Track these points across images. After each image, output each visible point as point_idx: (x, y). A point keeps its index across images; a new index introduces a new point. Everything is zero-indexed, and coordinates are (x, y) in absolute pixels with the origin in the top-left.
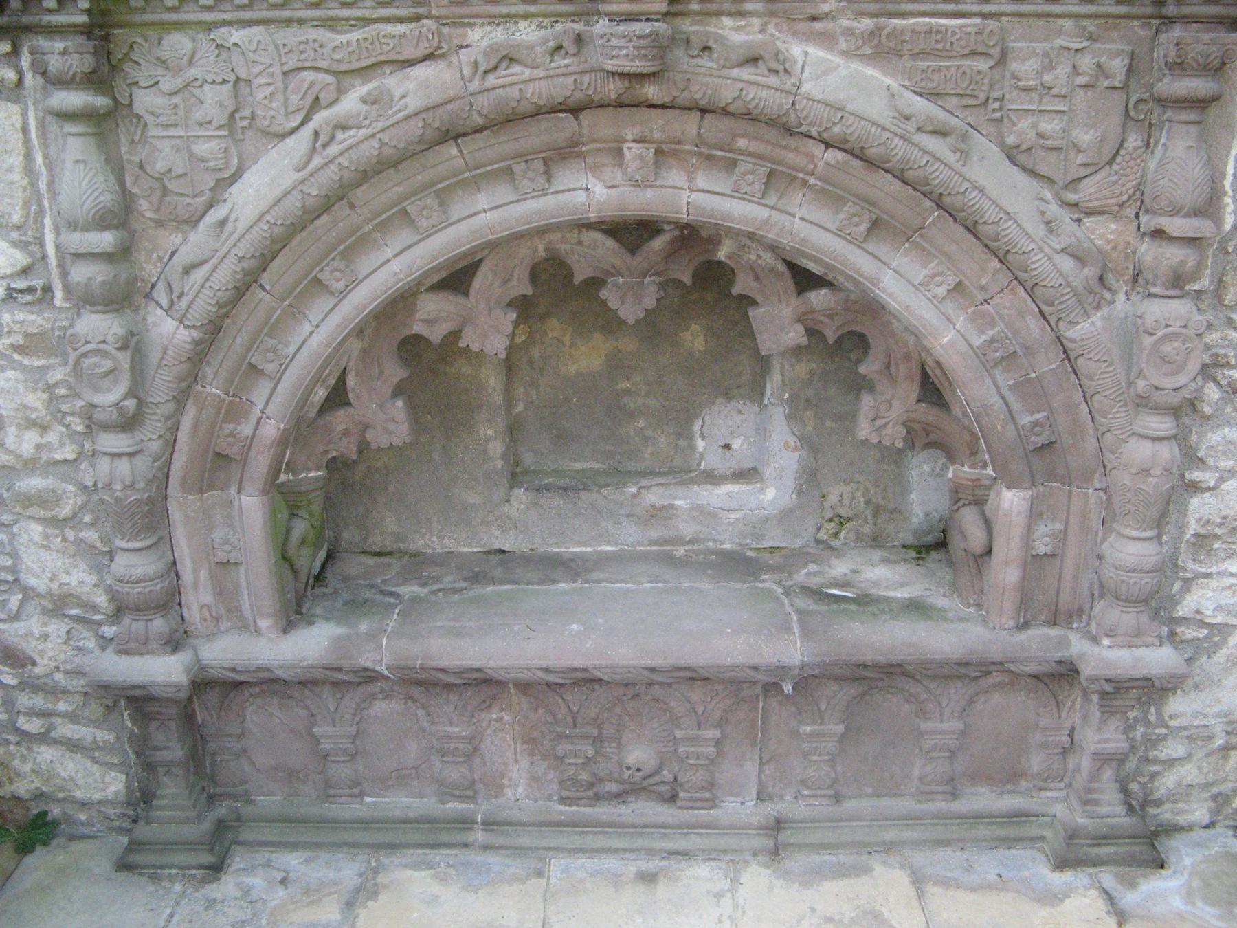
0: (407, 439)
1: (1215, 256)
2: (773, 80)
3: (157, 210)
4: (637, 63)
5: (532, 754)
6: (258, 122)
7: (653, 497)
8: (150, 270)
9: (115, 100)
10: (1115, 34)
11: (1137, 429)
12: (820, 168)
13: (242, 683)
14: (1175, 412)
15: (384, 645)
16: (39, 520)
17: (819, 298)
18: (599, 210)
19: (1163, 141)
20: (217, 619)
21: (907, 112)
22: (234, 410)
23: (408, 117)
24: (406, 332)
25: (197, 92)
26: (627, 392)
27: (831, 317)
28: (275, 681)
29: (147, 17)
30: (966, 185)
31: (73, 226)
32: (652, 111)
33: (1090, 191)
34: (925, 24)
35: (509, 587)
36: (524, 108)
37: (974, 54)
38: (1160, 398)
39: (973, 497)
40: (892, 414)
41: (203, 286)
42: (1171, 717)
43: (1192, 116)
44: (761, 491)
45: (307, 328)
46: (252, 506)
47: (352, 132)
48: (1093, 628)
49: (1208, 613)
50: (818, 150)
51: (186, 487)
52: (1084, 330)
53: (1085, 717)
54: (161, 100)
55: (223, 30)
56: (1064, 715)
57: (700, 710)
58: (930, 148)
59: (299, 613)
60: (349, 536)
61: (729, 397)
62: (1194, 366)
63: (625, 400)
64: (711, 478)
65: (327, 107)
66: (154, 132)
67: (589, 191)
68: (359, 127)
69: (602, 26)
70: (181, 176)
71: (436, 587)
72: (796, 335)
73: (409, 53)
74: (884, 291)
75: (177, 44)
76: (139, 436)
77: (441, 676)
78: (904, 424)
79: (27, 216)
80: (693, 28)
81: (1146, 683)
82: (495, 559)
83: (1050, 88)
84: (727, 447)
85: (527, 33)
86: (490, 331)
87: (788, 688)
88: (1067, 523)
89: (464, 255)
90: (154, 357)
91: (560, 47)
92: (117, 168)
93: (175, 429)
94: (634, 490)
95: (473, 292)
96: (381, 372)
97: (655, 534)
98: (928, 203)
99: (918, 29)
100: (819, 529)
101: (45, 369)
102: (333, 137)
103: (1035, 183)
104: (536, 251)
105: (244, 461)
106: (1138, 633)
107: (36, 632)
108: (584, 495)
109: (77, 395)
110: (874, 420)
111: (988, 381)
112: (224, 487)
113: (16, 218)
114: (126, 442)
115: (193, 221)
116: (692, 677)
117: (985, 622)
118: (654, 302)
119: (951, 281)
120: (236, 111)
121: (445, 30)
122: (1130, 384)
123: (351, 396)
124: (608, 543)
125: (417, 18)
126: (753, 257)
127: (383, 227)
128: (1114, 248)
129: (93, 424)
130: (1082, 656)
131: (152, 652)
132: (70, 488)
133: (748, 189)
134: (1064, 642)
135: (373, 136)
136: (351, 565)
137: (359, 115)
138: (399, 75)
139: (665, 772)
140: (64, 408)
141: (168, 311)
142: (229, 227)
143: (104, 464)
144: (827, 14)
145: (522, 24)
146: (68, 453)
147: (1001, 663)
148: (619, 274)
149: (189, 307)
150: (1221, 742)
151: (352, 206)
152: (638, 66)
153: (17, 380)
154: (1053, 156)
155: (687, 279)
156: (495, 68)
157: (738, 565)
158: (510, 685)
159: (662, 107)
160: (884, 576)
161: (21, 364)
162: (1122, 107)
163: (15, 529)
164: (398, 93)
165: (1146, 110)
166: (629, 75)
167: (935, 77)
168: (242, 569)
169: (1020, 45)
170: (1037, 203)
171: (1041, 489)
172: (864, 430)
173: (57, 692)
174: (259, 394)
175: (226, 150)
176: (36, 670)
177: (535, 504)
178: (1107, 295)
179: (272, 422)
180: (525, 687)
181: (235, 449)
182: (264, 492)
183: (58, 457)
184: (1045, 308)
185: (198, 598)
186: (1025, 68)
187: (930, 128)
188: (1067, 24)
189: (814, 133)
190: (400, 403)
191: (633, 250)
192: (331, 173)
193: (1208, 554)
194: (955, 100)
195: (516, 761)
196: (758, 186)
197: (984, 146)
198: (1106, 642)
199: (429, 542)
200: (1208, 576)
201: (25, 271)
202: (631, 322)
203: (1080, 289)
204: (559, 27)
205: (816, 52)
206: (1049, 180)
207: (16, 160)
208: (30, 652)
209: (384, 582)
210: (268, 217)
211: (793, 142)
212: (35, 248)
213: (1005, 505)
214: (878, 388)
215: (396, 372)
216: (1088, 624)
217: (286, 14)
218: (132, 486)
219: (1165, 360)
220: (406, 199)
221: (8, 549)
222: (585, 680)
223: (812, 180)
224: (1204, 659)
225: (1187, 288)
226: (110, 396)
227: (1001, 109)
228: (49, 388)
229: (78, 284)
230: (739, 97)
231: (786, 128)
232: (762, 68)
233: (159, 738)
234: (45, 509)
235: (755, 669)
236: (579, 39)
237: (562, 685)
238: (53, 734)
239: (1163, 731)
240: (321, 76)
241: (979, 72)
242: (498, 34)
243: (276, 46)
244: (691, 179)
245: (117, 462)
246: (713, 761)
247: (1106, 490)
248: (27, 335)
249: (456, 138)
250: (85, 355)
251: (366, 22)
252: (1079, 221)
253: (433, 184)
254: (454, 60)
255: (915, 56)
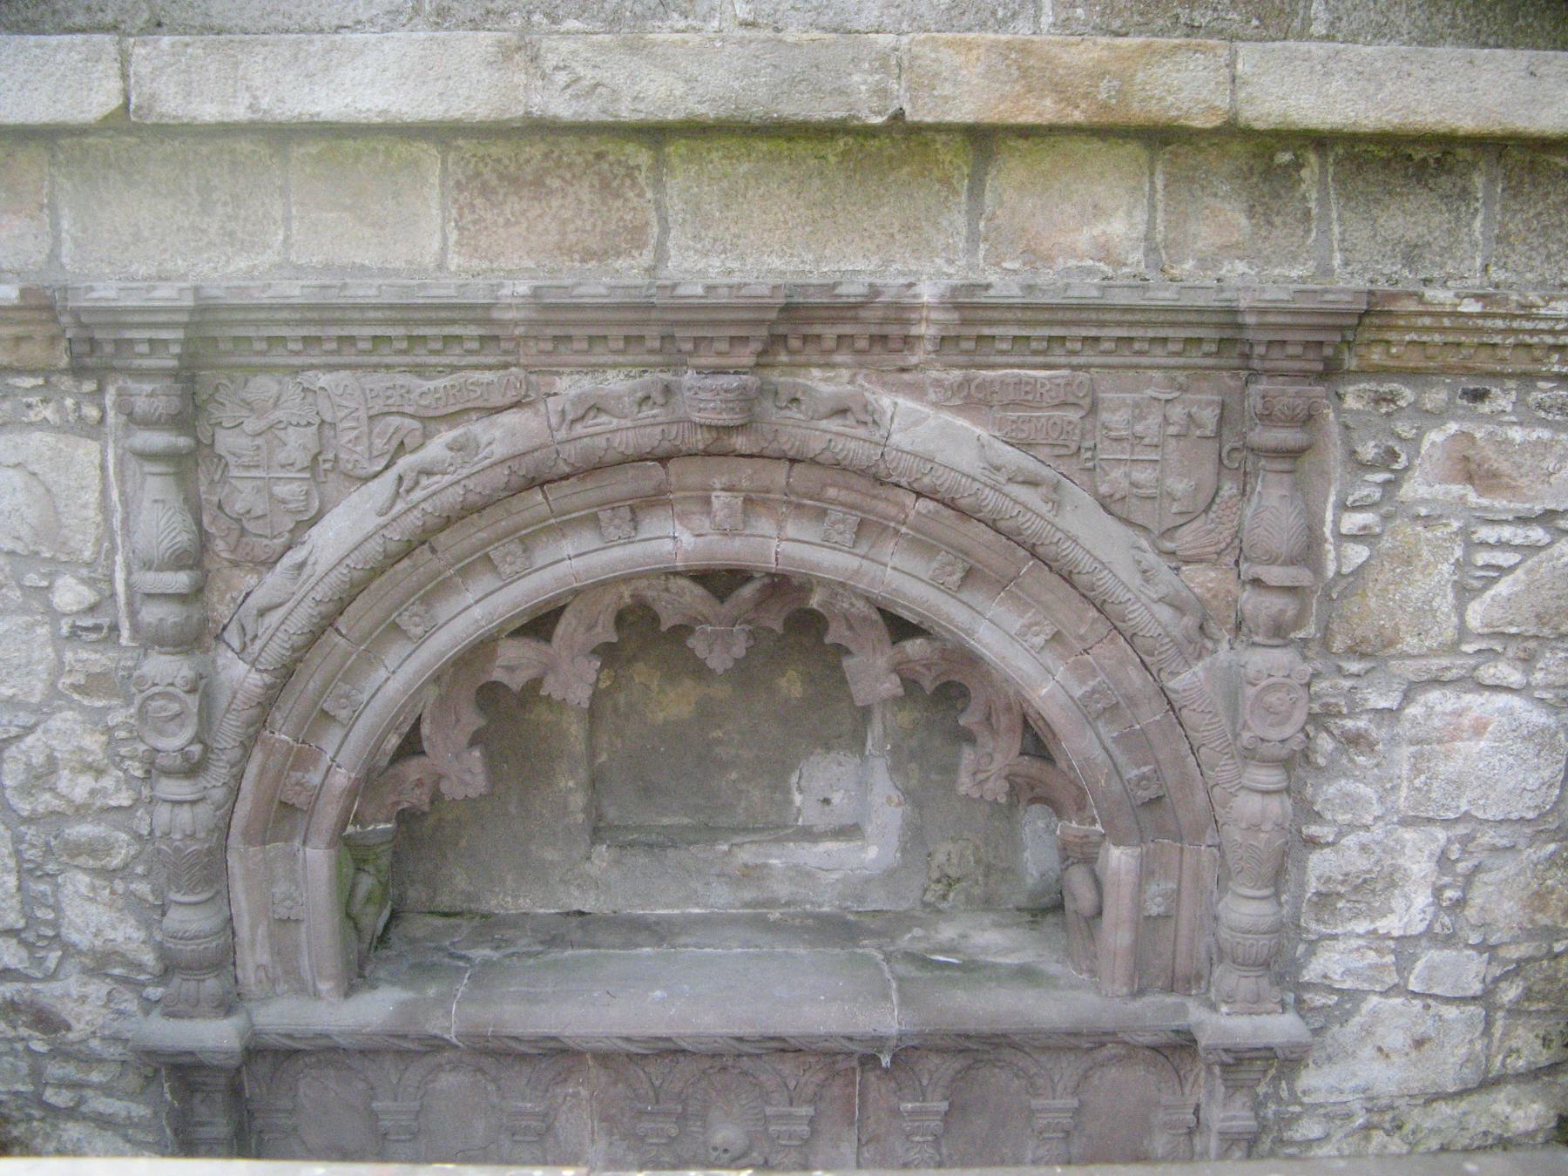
0: (483, 790)
1: (1320, 603)
2: (861, 432)
3: (232, 552)
4: (725, 416)
5: (610, 1133)
6: (342, 465)
7: (746, 855)
8: (223, 611)
9: (198, 442)
10: (1205, 385)
11: (1246, 782)
12: (911, 518)
13: (297, 1051)
14: (1285, 763)
15: (453, 1013)
16: (85, 870)
17: (914, 647)
18: (687, 560)
19: (1259, 489)
20: (274, 981)
21: (998, 462)
22: (302, 758)
23: (492, 466)
24: (484, 679)
25: (281, 434)
26: (718, 742)
27: (928, 667)
28: (335, 1049)
29: (233, 360)
30: (1059, 535)
31: (148, 565)
32: (741, 460)
33: (1186, 539)
34: (1015, 376)
35: (589, 951)
36: (611, 456)
37: (1064, 404)
38: (1264, 749)
39: (1082, 855)
40: (994, 767)
41: (277, 629)
42: (1304, 1093)
43: (1285, 466)
44: (863, 849)
45: (383, 673)
46: (317, 859)
47: (437, 478)
48: (1213, 995)
49: (1336, 977)
50: (909, 499)
51: (248, 839)
52: (1187, 680)
53: (1211, 1093)
54: (244, 441)
55: (310, 373)
56: (1187, 1091)
57: (792, 1084)
58: (1022, 498)
59: (361, 976)
60: (416, 894)
61: (828, 748)
62: (1300, 716)
63: (717, 750)
64: (809, 835)
65: (411, 452)
66: (234, 472)
67: (675, 539)
68: (444, 473)
69: (689, 378)
70: (258, 518)
71: (512, 950)
72: (891, 686)
73: (496, 400)
74: (979, 641)
75: (263, 387)
76: (202, 782)
77: (513, 1044)
78: (1006, 778)
79: (99, 553)
80: (782, 379)
81: (1268, 1054)
82: (575, 921)
83: (1142, 438)
84: (827, 801)
85: (615, 383)
86: (573, 677)
87: (886, 1060)
88: (1180, 882)
89: (547, 602)
90: (223, 702)
91: (648, 398)
92: (195, 509)
93: (239, 777)
94: (725, 847)
95: (556, 640)
96: (458, 721)
97: (748, 895)
98: (1022, 553)
99: (1008, 380)
100: (926, 890)
101: (107, 709)
102: (417, 483)
103: (1130, 532)
104: (621, 597)
105: (310, 811)
106: (1258, 999)
107: (75, 992)
108: (671, 853)
109: (142, 741)
110: (974, 774)
111: (1090, 734)
112: (289, 839)
113: (87, 555)
114: (188, 790)
115: (270, 563)
116: (782, 1047)
117: (1098, 990)
118: (744, 652)
119: (1049, 630)
120: (320, 453)
121: (533, 378)
122: (1236, 736)
123: (426, 745)
124: (697, 905)
125: (506, 366)
126: (846, 605)
127: (465, 572)
128: (1215, 596)
129: (154, 769)
130: (1199, 1024)
131: (203, 1016)
132: (123, 836)
133: (837, 538)
134: (1181, 1010)
135: (458, 482)
136: (419, 926)
137: (444, 461)
138: (486, 422)
139: (755, 1154)
140: (123, 751)
141: (241, 653)
142: (307, 571)
143: (163, 813)
144: (916, 366)
145: (611, 374)
146: (124, 799)
147: (1114, 1033)
148: (707, 621)
149: (262, 650)
150: (1361, 1121)
151: (433, 551)
152: (725, 419)
153: (75, 721)
154: (1148, 505)
155: (778, 627)
156: (583, 418)
157: (836, 929)
158: (588, 1056)
159: (751, 456)
160: (994, 941)
161: (80, 705)
162: (1215, 456)
163: (60, 880)
164: (484, 440)
165: (1237, 459)
166: (717, 428)
167: (1025, 427)
168: (303, 928)
169: (1110, 395)
170: (1134, 552)
171: (1152, 846)
172: (965, 784)
173: (91, 1060)
174: (330, 741)
175: (307, 493)
176: (71, 1036)
177: (617, 862)
178: (1209, 644)
179: (343, 771)
180: (604, 1058)
181: (302, 798)
182: (330, 845)
183: (113, 803)
184: (1146, 659)
185: (254, 957)
186: (1116, 419)
187: (1020, 479)
188: (1157, 375)
189: (904, 482)
190: (477, 753)
191: (722, 598)
192: (414, 519)
193: (1332, 914)
194: (1047, 450)
195: (593, 1141)
196: (849, 536)
197: (1077, 494)
198: (1224, 1009)
199: (501, 902)
200: (1334, 937)
201: (92, 609)
202: (720, 671)
203: (1180, 638)
204: (647, 376)
205: (905, 403)
206: (1145, 528)
207: (92, 497)
208: (64, 1015)
209: (453, 944)
210: (348, 561)
211: (882, 492)
212: (104, 586)
213: (1113, 863)
214: (980, 740)
215: (473, 720)
216: (1208, 990)
217: (375, 359)
218: (192, 836)
219: (1269, 710)
220: (489, 544)
221: (51, 900)
222: (669, 1051)
223: (904, 530)
224: (1336, 1028)
225: (1292, 635)
226: (175, 741)
227: (1093, 458)
228: (109, 730)
229: (149, 624)
230: (827, 448)
231: (878, 478)
232: (851, 420)
233: (202, 1112)
234: (94, 858)
235: (850, 1039)
236: (667, 390)
237: (645, 1056)
238: (84, 1109)
239: (1297, 1109)
240: (407, 421)
241: (1070, 423)
242: (586, 383)
243: (363, 390)
244: (780, 528)
245: (177, 809)
246: (806, 1142)
247: (1219, 847)
248: (88, 675)
249: (541, 485)
250: (151, 698)
251: (455, 369)
252: (1177, 569)
253: (517, 530)
254: (542, 408)
255: (1005, 406)
